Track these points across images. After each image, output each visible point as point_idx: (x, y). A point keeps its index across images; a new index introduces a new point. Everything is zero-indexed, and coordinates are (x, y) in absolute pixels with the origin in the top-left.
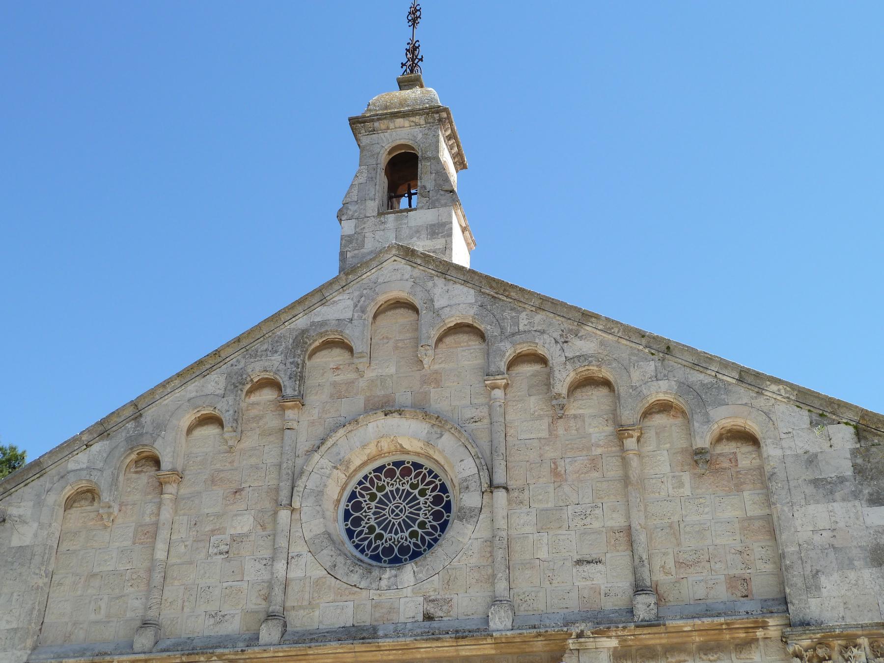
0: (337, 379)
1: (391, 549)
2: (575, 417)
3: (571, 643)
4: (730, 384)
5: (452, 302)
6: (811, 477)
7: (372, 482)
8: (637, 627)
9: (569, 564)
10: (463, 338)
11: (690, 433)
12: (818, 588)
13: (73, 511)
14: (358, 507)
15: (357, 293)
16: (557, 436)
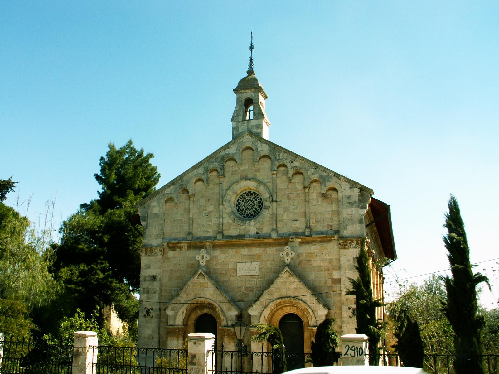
0: (233, 169)
1: (248, 214)
2: (294, 182)
3: (290, 240)
4: (332, 176)
5: (263, 149)
6: (348, 201)
7: (243, 197)
8: (305, 237)
9: (291, 221)
10: (265, 159)
11: (322, 189)
12: (347, 229)
13: (167, 203)
14: (239, 203)
15: (237, 145)
16: (289, 188)
